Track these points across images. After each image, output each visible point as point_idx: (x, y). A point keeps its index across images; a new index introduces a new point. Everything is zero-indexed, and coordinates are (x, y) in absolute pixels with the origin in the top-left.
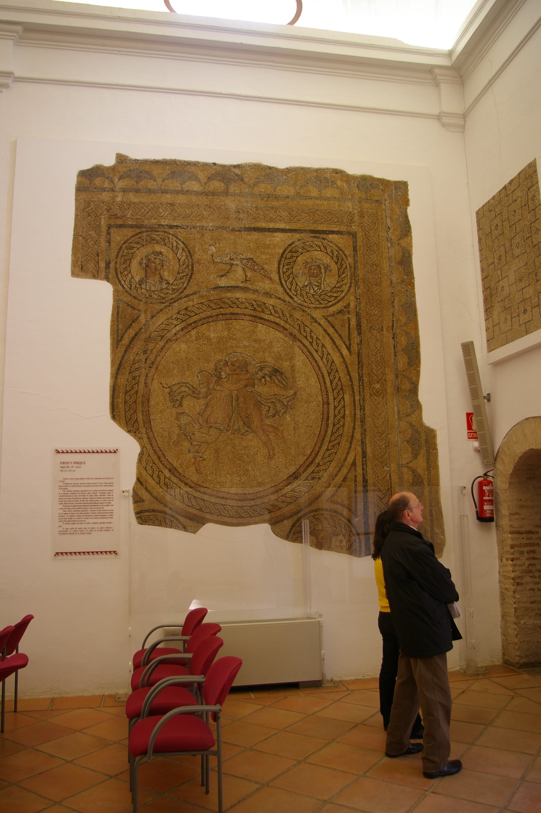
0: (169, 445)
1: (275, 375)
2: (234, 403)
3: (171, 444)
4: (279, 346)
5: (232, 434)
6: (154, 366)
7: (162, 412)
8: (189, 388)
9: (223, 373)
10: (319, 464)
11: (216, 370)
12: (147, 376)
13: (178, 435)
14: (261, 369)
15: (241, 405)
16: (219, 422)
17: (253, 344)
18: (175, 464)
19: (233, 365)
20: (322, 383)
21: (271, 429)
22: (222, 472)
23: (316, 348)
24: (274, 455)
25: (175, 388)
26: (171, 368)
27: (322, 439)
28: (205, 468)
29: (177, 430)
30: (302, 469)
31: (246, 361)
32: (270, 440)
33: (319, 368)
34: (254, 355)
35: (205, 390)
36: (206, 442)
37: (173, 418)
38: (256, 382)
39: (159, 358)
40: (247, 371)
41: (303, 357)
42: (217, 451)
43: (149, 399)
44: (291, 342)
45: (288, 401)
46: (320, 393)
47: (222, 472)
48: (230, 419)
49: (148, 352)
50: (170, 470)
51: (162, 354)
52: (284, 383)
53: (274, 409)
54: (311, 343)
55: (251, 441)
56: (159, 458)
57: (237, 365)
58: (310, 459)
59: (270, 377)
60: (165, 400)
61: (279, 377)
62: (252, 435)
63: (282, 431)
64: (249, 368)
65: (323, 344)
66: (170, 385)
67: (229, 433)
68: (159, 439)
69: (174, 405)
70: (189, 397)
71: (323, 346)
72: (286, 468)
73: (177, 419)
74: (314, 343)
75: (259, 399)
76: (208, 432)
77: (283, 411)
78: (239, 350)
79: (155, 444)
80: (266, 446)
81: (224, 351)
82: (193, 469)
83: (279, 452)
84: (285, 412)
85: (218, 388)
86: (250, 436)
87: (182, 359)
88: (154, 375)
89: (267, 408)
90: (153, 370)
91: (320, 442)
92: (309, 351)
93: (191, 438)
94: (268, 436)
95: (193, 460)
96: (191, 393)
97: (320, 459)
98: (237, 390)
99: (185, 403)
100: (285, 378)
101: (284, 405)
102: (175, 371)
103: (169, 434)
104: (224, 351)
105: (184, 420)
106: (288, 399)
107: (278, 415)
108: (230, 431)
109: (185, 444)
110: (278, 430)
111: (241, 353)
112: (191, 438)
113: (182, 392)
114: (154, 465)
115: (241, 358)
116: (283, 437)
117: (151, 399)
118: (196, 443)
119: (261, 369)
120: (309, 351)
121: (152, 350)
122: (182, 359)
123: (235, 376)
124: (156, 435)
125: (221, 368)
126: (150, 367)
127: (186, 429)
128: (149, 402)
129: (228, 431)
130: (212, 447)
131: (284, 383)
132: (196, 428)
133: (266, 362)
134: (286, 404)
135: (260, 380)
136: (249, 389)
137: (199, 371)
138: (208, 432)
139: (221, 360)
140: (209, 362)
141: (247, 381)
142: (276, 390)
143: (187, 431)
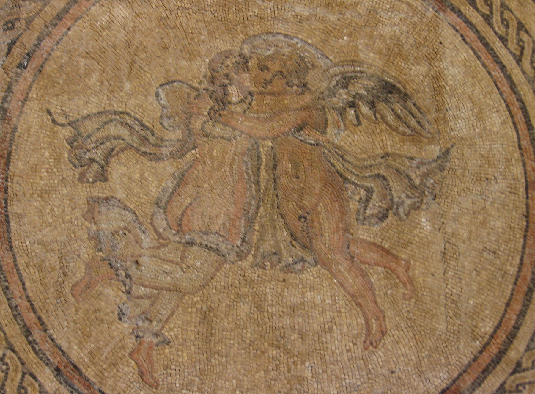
0: (59, 293)
1: (386, 101)
2: (263, 174)
3: (67, 290)
4: (397, 20)
5: (253, 265)
6: (34, 64)
7: (44, 194)
8: (131, 128)
9: (232, 90)
10: (519, 364)
11: (212, 80)
12: (9, 89)
13: (88, 266)
14: (346, 81)
15: (283, 180)
16: (215, 228)
17: (321, 12)
18: (77, 354)
19: (263, 68)
20: (522, 127)
21: (372, 256)
22: (220, 383)
23: (501, 31)
24: (383, 333)
25: (90, 126)
26: (82, 71)
27: (525, 288)
28: (167, 367)
29: (85, 250)
30: (469, 380)
31: (302, 58)
32: (371, 288)
33: (513, 86)
34: (324, 41)
35: (178, 134)
36: (174, 289)
37: (78, 213)
38: (332, 117)
39: (47, 43)
40: (305, 85)
41: (465, 53)
42: (207, 317)
43: (9, 154)
44: (431, 13)
45: (426, 175)
46: (517, 155)
47: (220, 383)
48: (250, 222)
49: (18, 25)
50: (58, 370)
51: (58, 32)
52: (413, 123)
53: (384, 196)
54: (487, 19)
55: (312, 288)
56: (27, 332)
57: (275, 67)
58: (494, 349)
59: (372, 105)
60: (58, 160)
61: (398, 107)
62: (314, 270)
63: (408, 263)
64: (311, 77)
65: (519, 23)
66: (73, 116)
67: (246, 264)
68: (31, 275)
69: (82, 175)
70: (129, 153)
71: (521, 26)
72: (420, 374)
73: (91, 215)
74: (496, 18)
75: (339, 166)
76: (183, 258)
77: (409, 202)
78: (281, 27)
79: (16, 289)
80: (359, 305)
81: (239, 28)
82: (129, 369)
83: (397, 327)
84: (416, 207)
85: (218, 130)
86: (311, 275)
87: (114, 47)
88: (30, 88)
89: (363, 193)
90: (28, 74)
91: (520, 297)
92: (482, 39)
93: (128, 276)
94: (364, 275)
95: (131, 342)
96: (135, 141)
97: (522, 348)
98: (274, 139)
99: (117, 170)
100: (414, 110)
101: (413, 187)
102: (93, 80)
103: (61, 259)
104: (239, 28)
105: (110, 220)
106: (423, 169)
107: (396, 214)
108: (250, 258)
109: (110, 292)
110: (396, 257)
111: (286, 36)
112: (128, 276)
113: (108, 138)
114: (9, 353)
115: (286, 50)
116: (411, 280)
117: (14, 157)
118: (142, 291)
119: (346, 81)
120: (482, 39)
121: (29, 22)
122: (114, 47)
123: (268, 99)
124: (21, 261)
125: (227, 76)
126: (21, 66)
127: (113, 248)
128: (8, 163)
129: (241, 256)
130: (194, 305)
131: (413, 123)
132: (145, 245)
133: (361, 64)
134: (417, 182)
135: (342, 112)
136: (310, 136)
137: (163, 81)
138: (183, 258)
139: (228, 54)
140: (192, 56)
141: (303, 114)
142: (390, 143)
143: (117, 252)
